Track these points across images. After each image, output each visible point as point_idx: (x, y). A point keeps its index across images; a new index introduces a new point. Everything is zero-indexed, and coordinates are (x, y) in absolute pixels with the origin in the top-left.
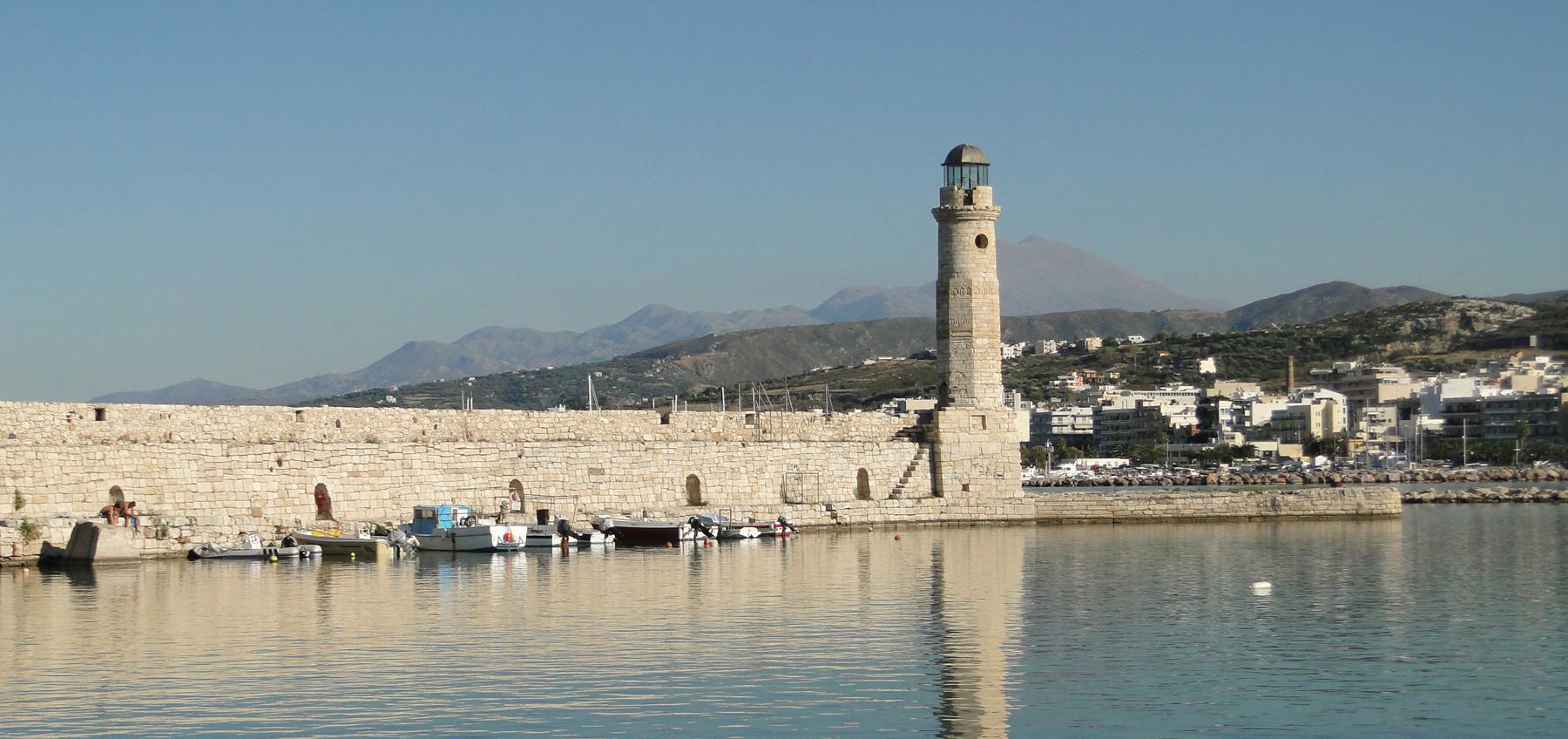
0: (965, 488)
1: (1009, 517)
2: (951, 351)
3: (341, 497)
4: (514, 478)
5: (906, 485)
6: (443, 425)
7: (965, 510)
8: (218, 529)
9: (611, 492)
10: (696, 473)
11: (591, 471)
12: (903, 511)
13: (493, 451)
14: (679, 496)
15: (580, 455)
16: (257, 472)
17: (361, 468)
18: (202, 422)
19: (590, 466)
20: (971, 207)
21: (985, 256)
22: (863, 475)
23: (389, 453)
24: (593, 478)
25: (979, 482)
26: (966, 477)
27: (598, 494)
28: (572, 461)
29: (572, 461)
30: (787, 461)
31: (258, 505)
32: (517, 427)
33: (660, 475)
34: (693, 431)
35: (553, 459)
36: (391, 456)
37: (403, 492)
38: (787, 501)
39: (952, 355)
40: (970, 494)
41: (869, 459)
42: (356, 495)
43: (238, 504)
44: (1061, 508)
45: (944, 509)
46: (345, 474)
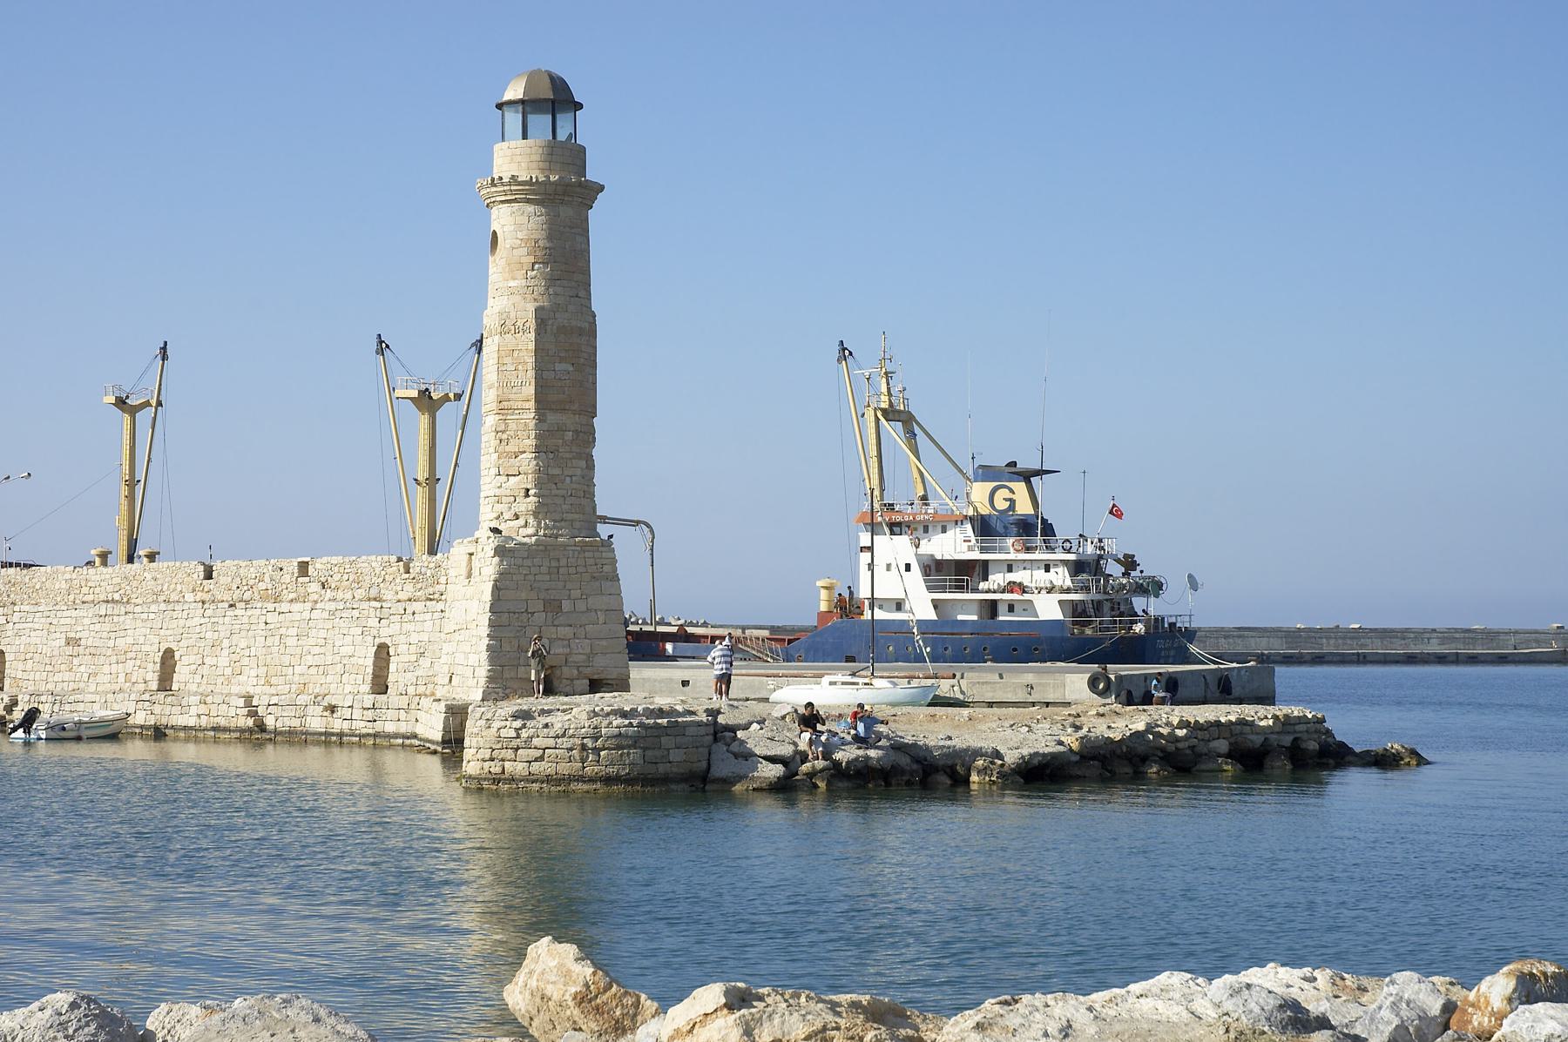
9: (82, 669)
14: (149, 676)
15: (63, 621)
22: (383, 654)
24: (69, 650)
30: (283, 631)
41: (395, 628)
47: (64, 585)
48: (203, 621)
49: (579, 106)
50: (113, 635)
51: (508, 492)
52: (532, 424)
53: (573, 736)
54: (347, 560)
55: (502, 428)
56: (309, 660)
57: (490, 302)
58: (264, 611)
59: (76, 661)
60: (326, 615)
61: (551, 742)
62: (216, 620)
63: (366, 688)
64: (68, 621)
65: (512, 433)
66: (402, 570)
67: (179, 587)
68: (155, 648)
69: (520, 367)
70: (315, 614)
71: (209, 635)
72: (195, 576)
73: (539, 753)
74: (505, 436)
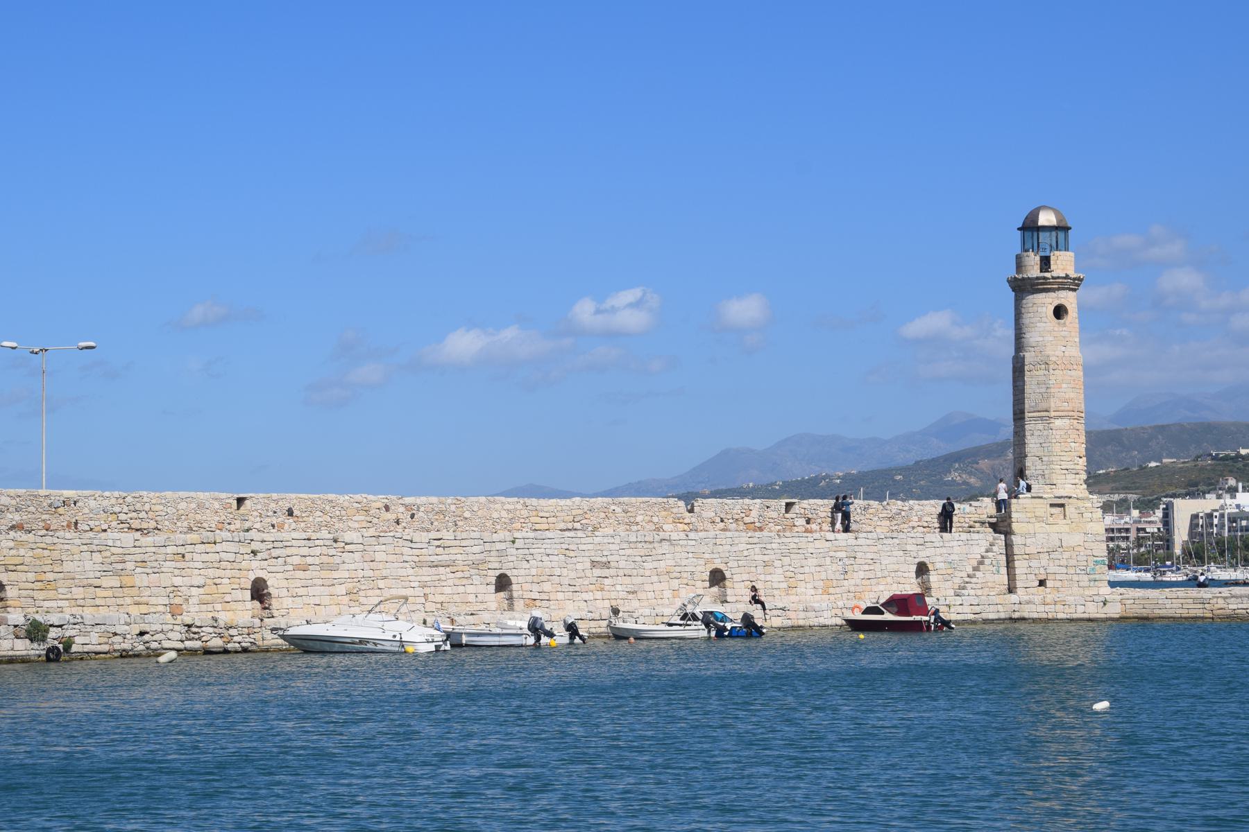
0: (1042, 583)
1: (1092, 616)
2: (1027, 433)
3: (284, 592)
4: (501, 571)
5: (973, 580)
6: (421, 514)
7: (1041, 608)
8: (112, 630)
9: (619, 588)
10: (722, 567)
11: (594, 564)
12: (967, 609)
13: (476, 542)
15: (582, 547)
16: (179, 565)
17: (309, 560)
18: (117, 509)
19: (593, 559)
20: (1047, 275)
21: (1064, 329)
23: (346, 544)
24: (597, 572)
25: (1058, 577)
26: (1042, 571)
27: (602, 590)
28: (572, 554)
29: (572, 554)
30: (832, 554)
31: (177, 601)
32: (511, 516)
33: (678, 569)
34: (722, 521)
35: (549, 551)
37: (363, 588)
38: (756, 600)
39: (1029, 437)
40: (1048, 590)
42: (302, 591)
43: (153, 600)
44: (1152, 606)
45: (1016, 607)
48: (749, 546)
59: (606, 581)
64: (590, 547)
70: (860, 542)
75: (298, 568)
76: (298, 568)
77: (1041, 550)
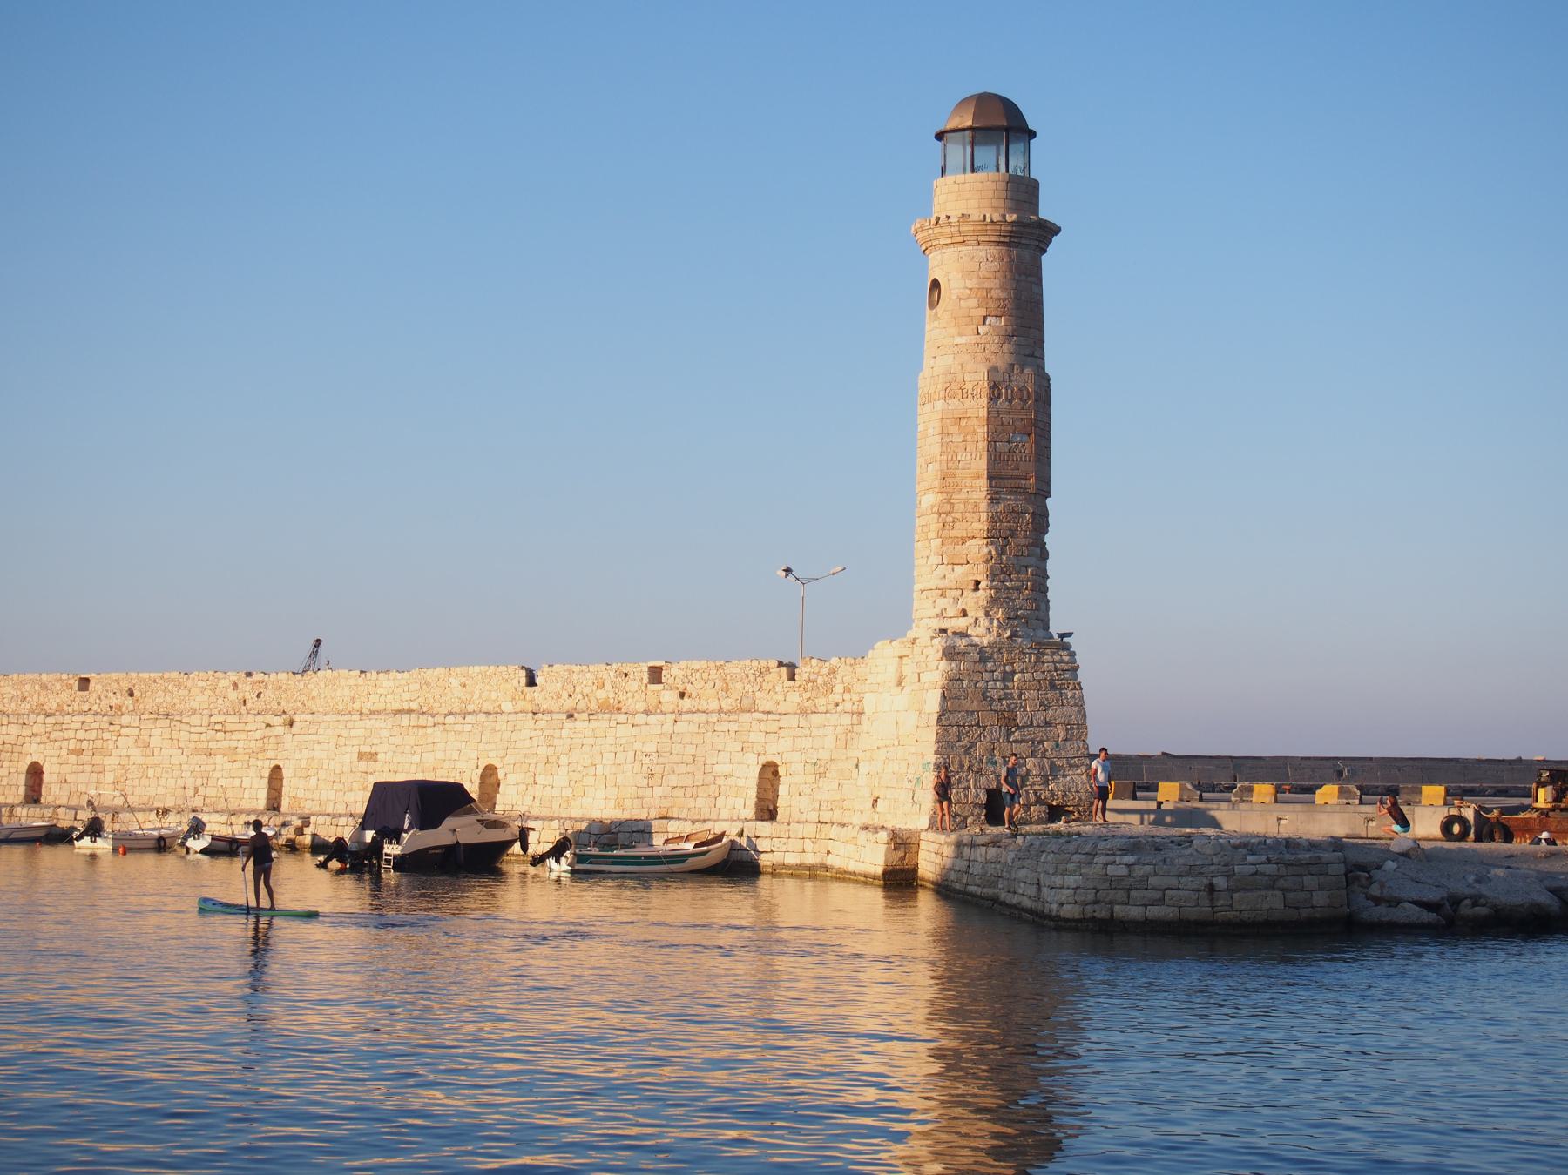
11: (361, 756)
15: (353, 733)
17: (85, 745)
22: (770, 773)
23: (122, 727)
24: (363, 765)
30: (638, 746)
36: (123, 731)
41: (785, 744)
46: (64, 752)
47: (347, 692)
48: (533, 734)
49: (1032, 134)
50: (418, 750)
51: (953, 585)
52: (984, 506)
53: (1201, 874)
54: (712, 664)
55: (947, 508)
56: (673, 780)
57: (928, 361)
58: (613, 723)
60: (693, 728)
61: (1173, 882)
62: (551, 732)
63: (749, 812)
65: (958, 515)
66: (785, 677)
67: (494, 695)
68: (473, 764)
69: (969, 438)
70: (681, 727)
71: (542, 750)
72: (515, 683)
73: (1158, 895)
74: (949, 519)
75: (71, 752)
76: (71, 752)
77: (880, 744)
